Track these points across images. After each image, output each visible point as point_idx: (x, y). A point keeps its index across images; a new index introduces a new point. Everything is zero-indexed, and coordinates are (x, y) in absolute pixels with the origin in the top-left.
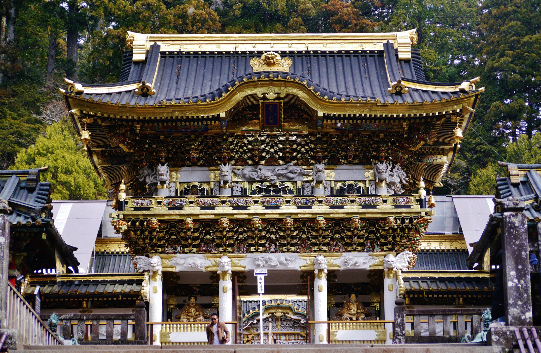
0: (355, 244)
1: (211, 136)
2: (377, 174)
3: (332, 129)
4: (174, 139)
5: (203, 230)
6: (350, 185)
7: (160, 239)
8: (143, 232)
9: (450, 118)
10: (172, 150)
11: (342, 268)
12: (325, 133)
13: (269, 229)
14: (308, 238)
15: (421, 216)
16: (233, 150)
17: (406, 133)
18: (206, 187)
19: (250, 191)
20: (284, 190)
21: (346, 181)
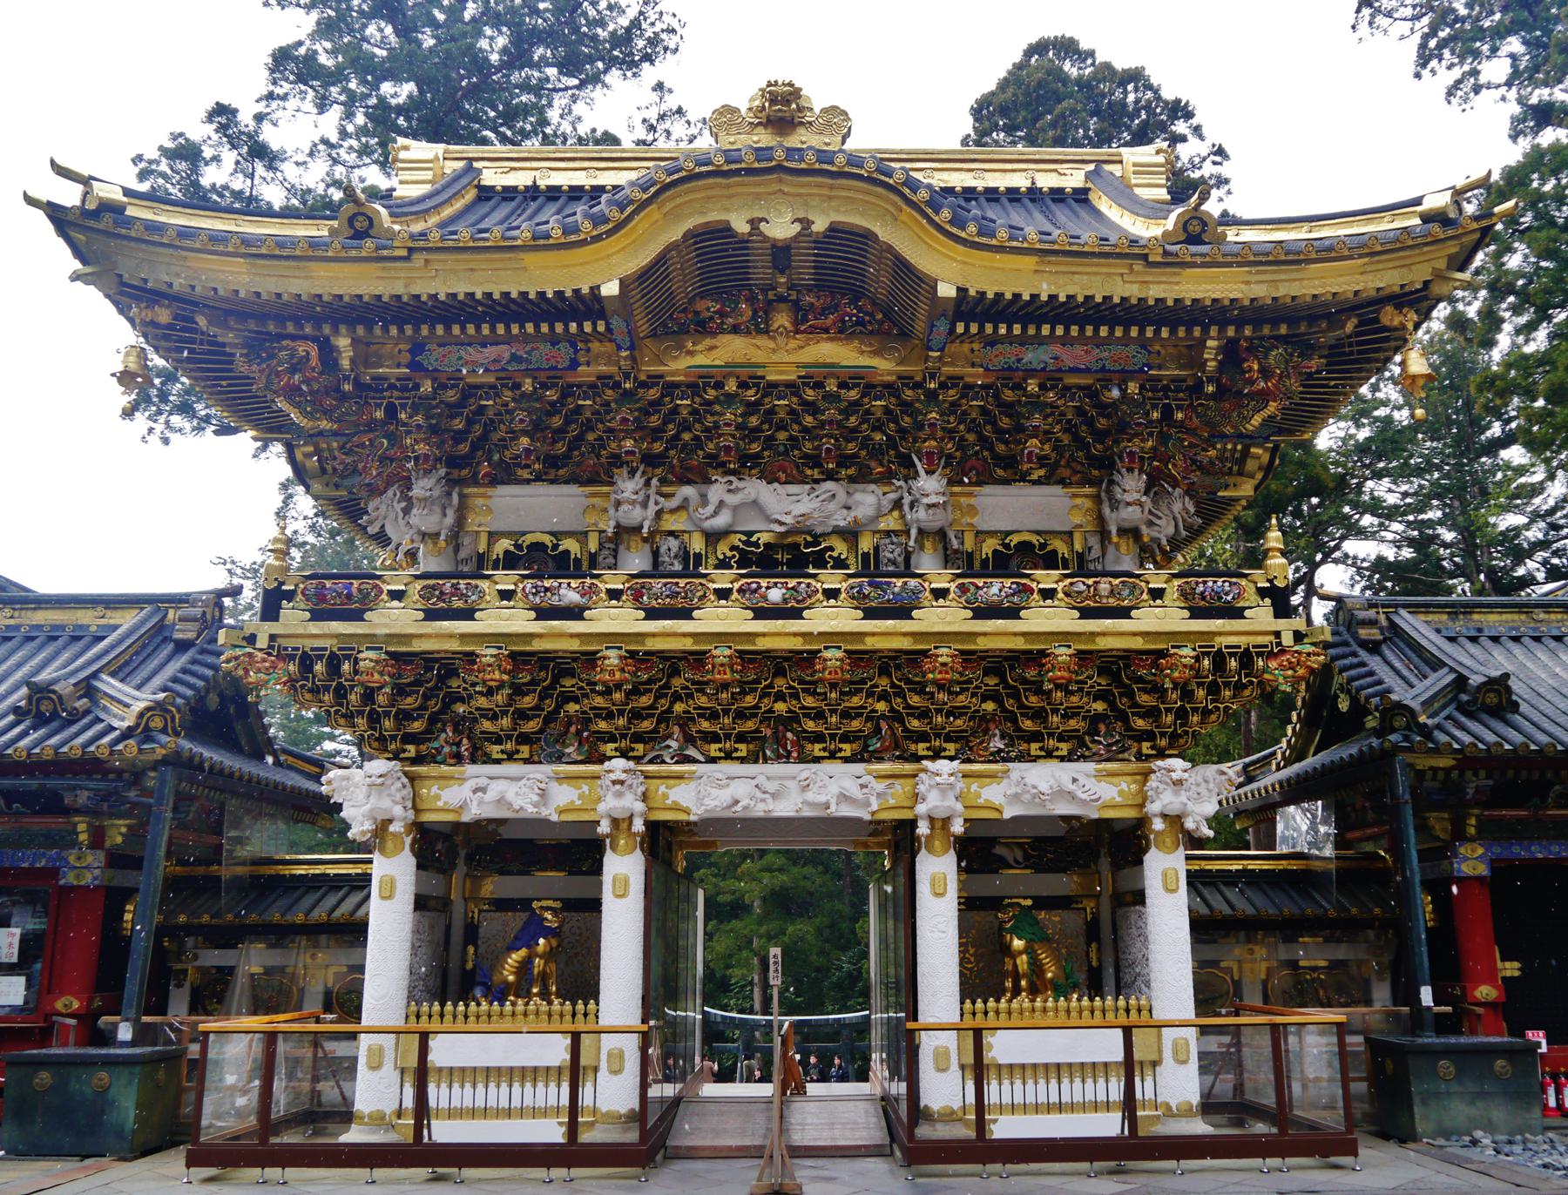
0: (1051, 735)
1: (592, 386)
2: (1107, 511)
3: (973, 365)
4: (471, 396)
5: (552, 687)
6: (1025, 546)
7: (404, 716)
8: (341, 694)
9: (1377, 320)
10: (467, 431)
11: (1007, 815)
12: (950, 378)
13: (771, 686)
14: (896, 717)
15: (1279, 644)
16: (656, 433)
17: (1210, 380)
18: (570, 545)
19: (712, 561)
20: (820, 562)
21: (1008, 533)
